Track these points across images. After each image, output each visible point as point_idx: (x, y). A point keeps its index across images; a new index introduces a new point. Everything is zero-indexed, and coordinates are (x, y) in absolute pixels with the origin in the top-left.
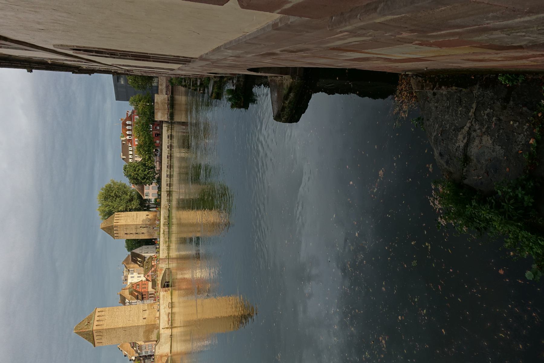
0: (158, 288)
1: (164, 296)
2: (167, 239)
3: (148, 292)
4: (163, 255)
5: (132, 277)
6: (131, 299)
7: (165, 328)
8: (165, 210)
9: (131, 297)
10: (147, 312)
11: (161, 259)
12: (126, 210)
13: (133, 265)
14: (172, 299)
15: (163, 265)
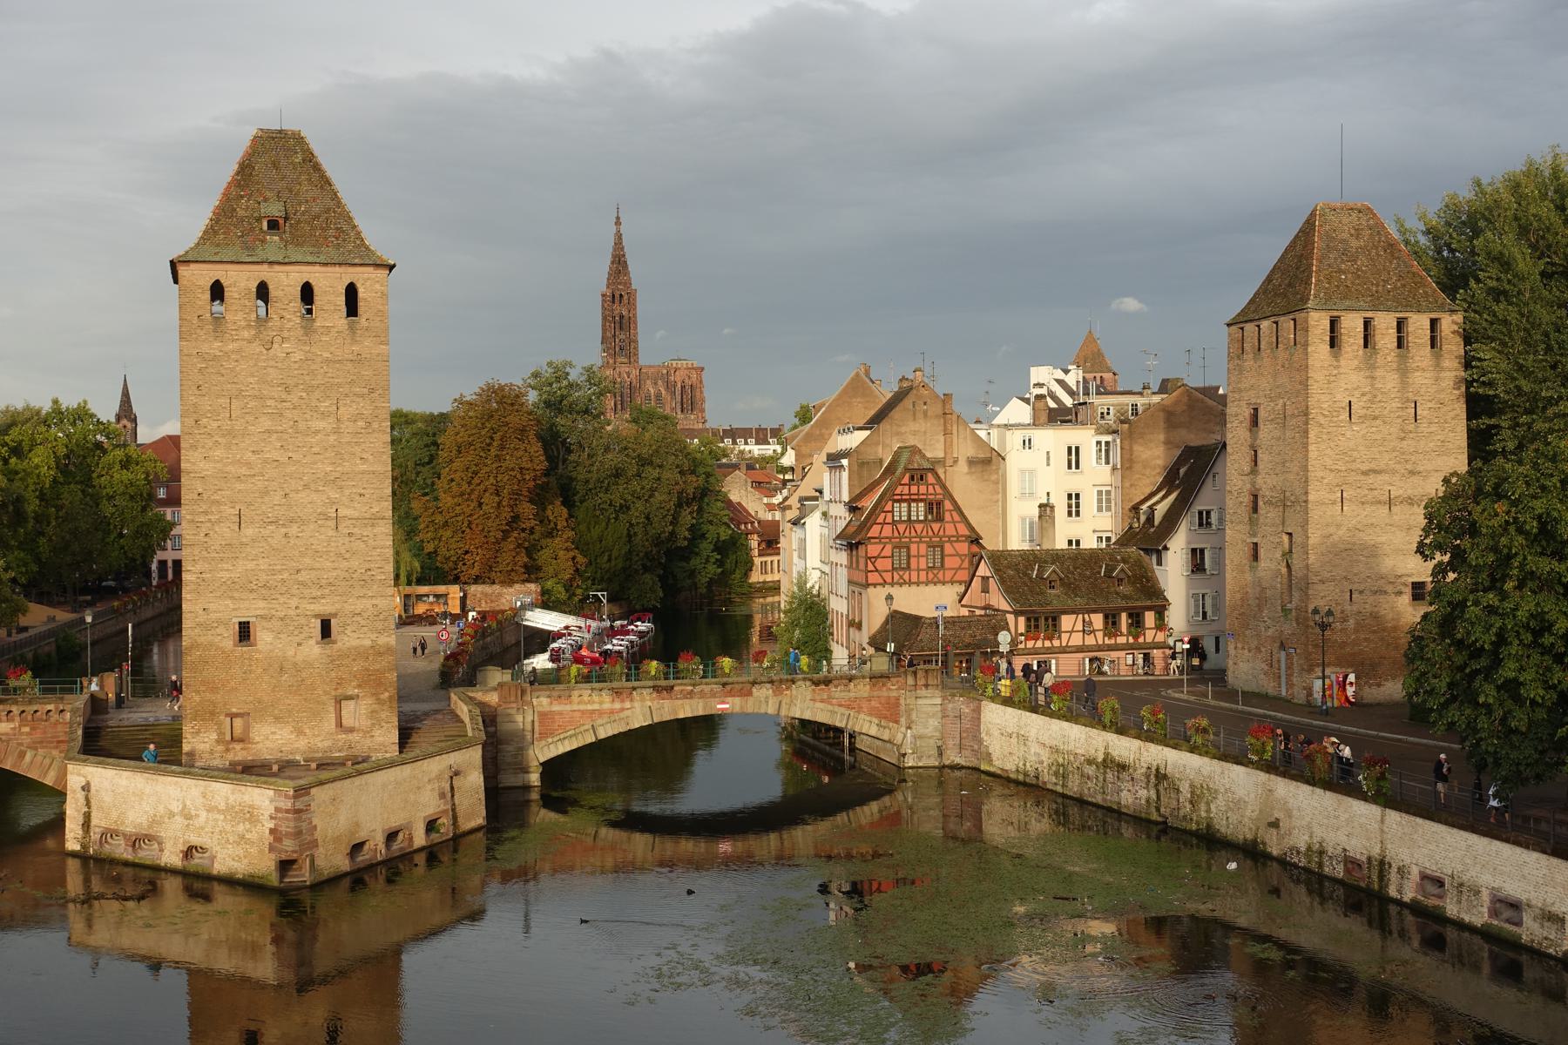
0: (702, 695)
1: (250, 815)
2: (1074, 786)
3: (867, 585)
4: (996, 733)
5: (1074, 457)
6: (862, 464)
7: (88, 804)
8: (1251, 812)
9: (881, 461)
10: (313, 649)
11: (978, 711)
12: (1477, 405)
13: (1155, 455)
14: (230, 881)
15: (934, 723)
